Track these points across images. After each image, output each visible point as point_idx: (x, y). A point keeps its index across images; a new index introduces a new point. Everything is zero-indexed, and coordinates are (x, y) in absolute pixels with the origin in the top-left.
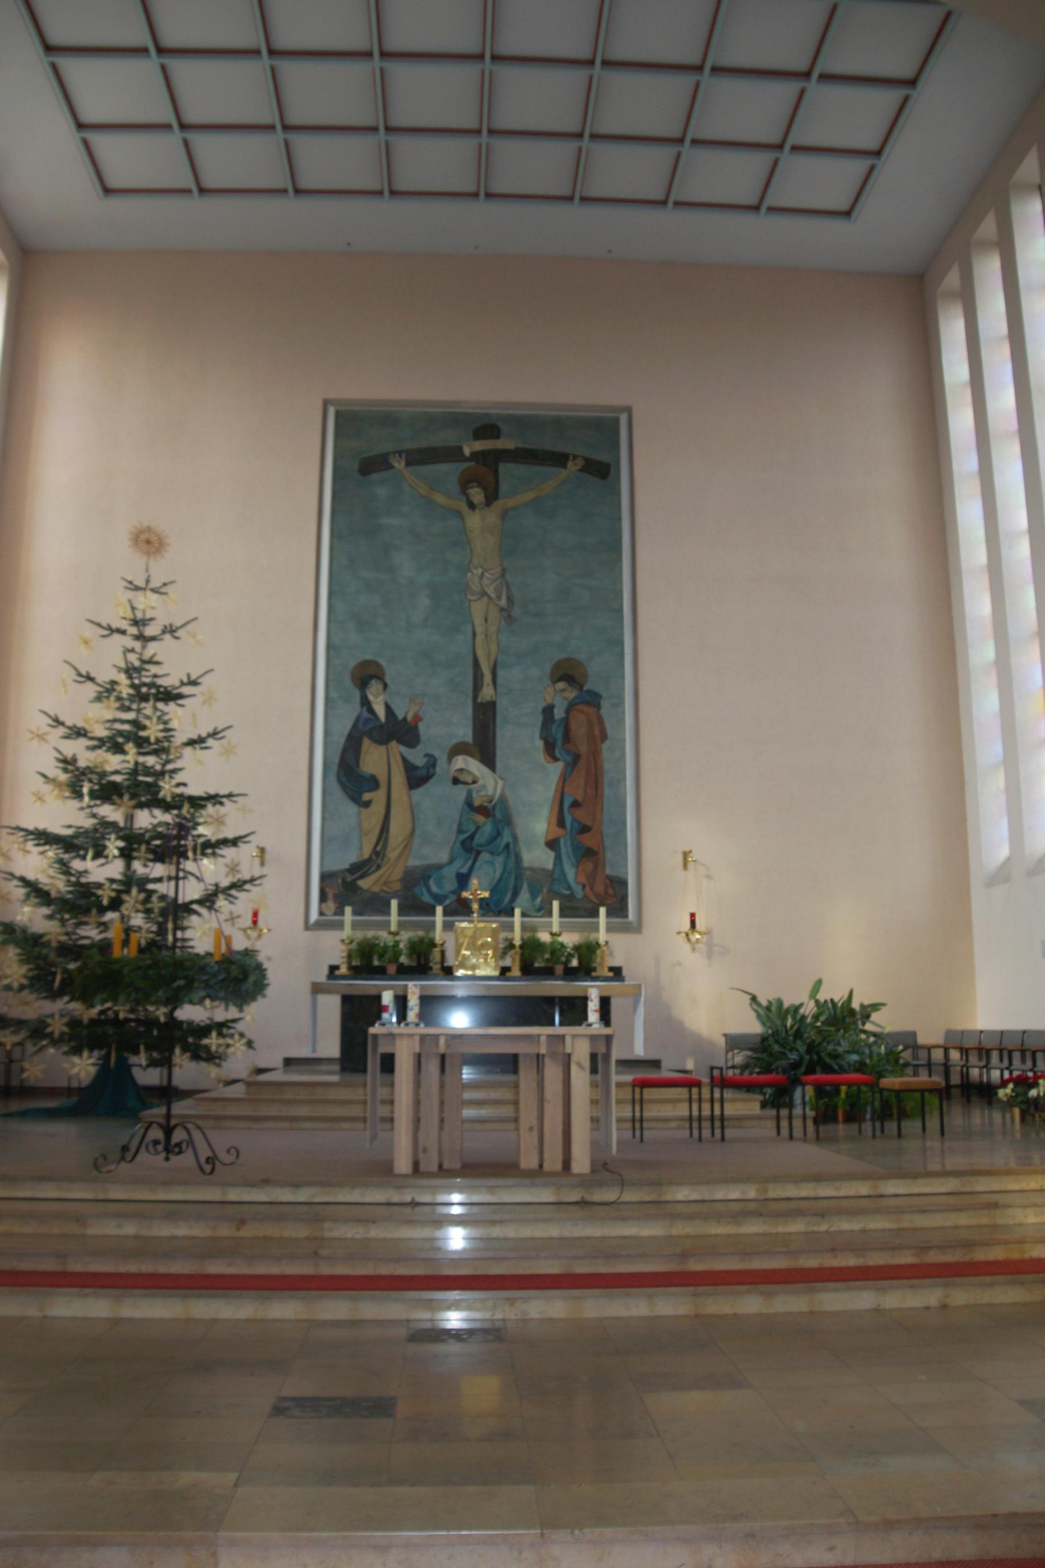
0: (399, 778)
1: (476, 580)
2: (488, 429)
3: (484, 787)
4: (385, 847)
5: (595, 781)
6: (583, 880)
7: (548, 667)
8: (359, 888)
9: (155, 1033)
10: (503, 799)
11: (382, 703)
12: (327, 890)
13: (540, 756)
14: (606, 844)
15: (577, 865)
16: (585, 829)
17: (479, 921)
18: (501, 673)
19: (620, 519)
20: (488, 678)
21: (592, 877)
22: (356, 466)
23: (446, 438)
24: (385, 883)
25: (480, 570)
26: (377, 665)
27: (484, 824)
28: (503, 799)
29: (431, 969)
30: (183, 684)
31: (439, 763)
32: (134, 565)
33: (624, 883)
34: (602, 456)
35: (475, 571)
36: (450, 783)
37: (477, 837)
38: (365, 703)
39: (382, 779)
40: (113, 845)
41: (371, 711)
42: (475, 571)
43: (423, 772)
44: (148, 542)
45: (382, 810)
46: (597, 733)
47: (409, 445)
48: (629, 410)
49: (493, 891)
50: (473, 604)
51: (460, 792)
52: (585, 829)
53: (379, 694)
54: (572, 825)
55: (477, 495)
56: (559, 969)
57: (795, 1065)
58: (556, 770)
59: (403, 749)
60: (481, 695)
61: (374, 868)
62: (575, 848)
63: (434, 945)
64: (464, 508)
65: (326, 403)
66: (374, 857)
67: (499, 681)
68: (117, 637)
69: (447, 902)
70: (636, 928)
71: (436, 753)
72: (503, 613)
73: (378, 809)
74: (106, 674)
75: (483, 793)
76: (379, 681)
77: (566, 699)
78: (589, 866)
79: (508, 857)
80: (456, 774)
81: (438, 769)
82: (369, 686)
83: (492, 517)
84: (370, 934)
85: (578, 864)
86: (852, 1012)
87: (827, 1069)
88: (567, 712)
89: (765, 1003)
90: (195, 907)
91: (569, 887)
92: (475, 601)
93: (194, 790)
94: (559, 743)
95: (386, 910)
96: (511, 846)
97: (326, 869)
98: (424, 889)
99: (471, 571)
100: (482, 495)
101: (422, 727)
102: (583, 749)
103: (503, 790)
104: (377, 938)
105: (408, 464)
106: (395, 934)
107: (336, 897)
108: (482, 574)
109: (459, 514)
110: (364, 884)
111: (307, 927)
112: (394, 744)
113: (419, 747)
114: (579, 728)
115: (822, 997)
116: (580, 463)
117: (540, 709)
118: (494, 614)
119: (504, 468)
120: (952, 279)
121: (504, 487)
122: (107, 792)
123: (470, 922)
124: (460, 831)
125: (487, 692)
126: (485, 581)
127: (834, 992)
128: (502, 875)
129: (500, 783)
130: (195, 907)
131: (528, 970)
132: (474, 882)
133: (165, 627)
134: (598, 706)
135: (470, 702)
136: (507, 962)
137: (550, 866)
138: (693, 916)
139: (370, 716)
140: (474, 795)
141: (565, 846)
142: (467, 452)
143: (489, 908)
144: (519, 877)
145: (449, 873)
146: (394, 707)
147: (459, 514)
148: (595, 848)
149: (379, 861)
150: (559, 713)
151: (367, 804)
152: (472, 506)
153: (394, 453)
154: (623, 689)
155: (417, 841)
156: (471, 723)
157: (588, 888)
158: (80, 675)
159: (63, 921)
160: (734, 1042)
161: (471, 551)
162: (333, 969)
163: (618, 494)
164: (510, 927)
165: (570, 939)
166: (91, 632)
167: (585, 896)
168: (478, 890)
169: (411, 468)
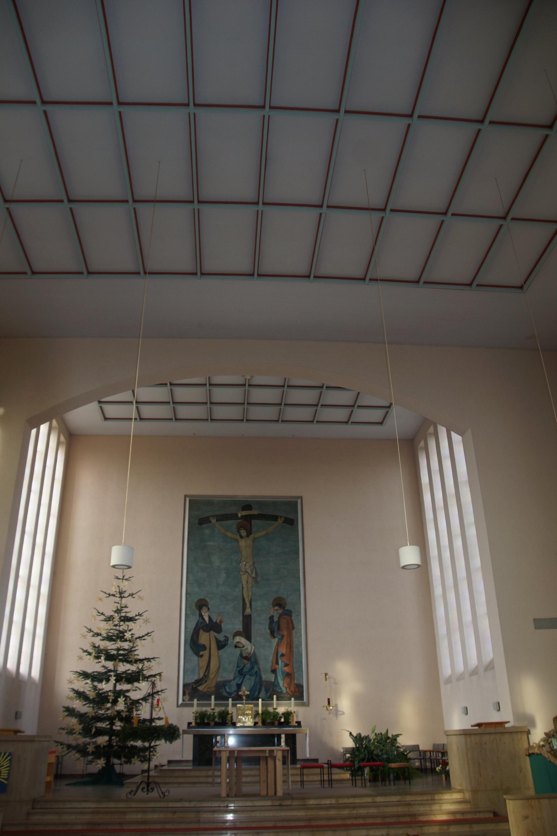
1: (243, 567)
2: (247, 506)
3: (247, 649)
4: (208, 673)
6: (286, 685)
7: (271, 601)
8: (198, 690)
9: (127, 751)
10: (254, 654)
11: (208, 615)
12: (186, 691)
13: (269, 636)
14: (295, 671)
17: (246, 704)
18: (253, 603)
19: (298, 541)
20: (248, 606)
22: (197, 522)
23: (231, 510)
24: (209, 688)
25: (245, 563)
27: (247, 663)
28: (254, 654)
29: (227, 723)
30: (136, 616)
31: (229, 639)
33: (302, 687)
34: (290, 517)
35: (243, 563)
36: (234, 648)
37: (244, 669)
38: (201, 616)
40: (113, 679)
41: (203, 619)
42: (243, 563)
47: (217, 513)
48: (301, 498)
49: (250, 691)
50: (242, 576)
51: (238, 651)
53: (206, 612)
54: (281, 663)
55: (244, 533)
56: (276, 723)
59: (215, 634)
60: (245, 612)
61: (204, 682)
63: (229, 714)
64: (238, 537)
65: (186, 496)
66: (204, 677)
67: (253, 607)
68: (111, 597)
69: (233, 695)
70: (307, 705)
71: (228, 636)
72: (254, 579)
73: (206, 658)
74: (109, 613)
75: (246, 651)
76: (206, 607)
77: (278, 613)
80: (236, 644)
81: (229, 642)
82: (203, 609)
83: (249, 541)
84: (204, 709)
85: (284, 679)
87: (374, 760)
88: (279, 618)
90: (141, 701)
91: (281, 689)
92: (244, 574)
93: (141, 657)
94: (276, 631)
95: (210, 699)
96: (258, 672)
97: (185, 682)
98: (224, 690)
99: (242, 563)
100: (246, 533)
101: (223, 625)
102: (285, 633)
103: (254, 650)
104: (206, 711)
105: (217, 521)
106: (213, 709)
108: (246, 564)
109: (237, 540)
110: (200, 688)
111: (178, 706)
112: (212, 632)
113: (222, 633)
115: (377, 731)
116: (283, 519)
117: (268, 617)
118: (250, 580)
119: (253, 522)
120: (422, 444)
121: (254, 529)
122: (110, 657)
123: (242, 704)
124: (238, 667)
125: (248, 611)
126: (247, 567)
128: (254, 684)
129: (253, 647)
130: (141, 701)
132: (244, 688)
133: (130, 594)
134: (291, 616)
135: (241, 615)
136: (257, 720)
137: (273, 680)
138: (329, 699)
139: (203, 621)
140: (243, 652)
142: (239, 515)
143: (249, 698)
144: (261, 685)
145: (234, 683)
146: (212, 617)
147: (237, 540)
149: (206, 679)
150: (276, 619)
151: (202, 656)
152: (242, 537)
153: (212, 516)
154: (300, 609)
155: (221, 671)
156: (241, 623)
157: (288, 689)
158: (99, 612)
159: (93, 707)
161: (241, 555)
162: (189, 724)
163: (297, 531)
164: (257, 705)
166: (103, 595)
167: (287, 692)
168: (245, 691)
169: (218, 522)
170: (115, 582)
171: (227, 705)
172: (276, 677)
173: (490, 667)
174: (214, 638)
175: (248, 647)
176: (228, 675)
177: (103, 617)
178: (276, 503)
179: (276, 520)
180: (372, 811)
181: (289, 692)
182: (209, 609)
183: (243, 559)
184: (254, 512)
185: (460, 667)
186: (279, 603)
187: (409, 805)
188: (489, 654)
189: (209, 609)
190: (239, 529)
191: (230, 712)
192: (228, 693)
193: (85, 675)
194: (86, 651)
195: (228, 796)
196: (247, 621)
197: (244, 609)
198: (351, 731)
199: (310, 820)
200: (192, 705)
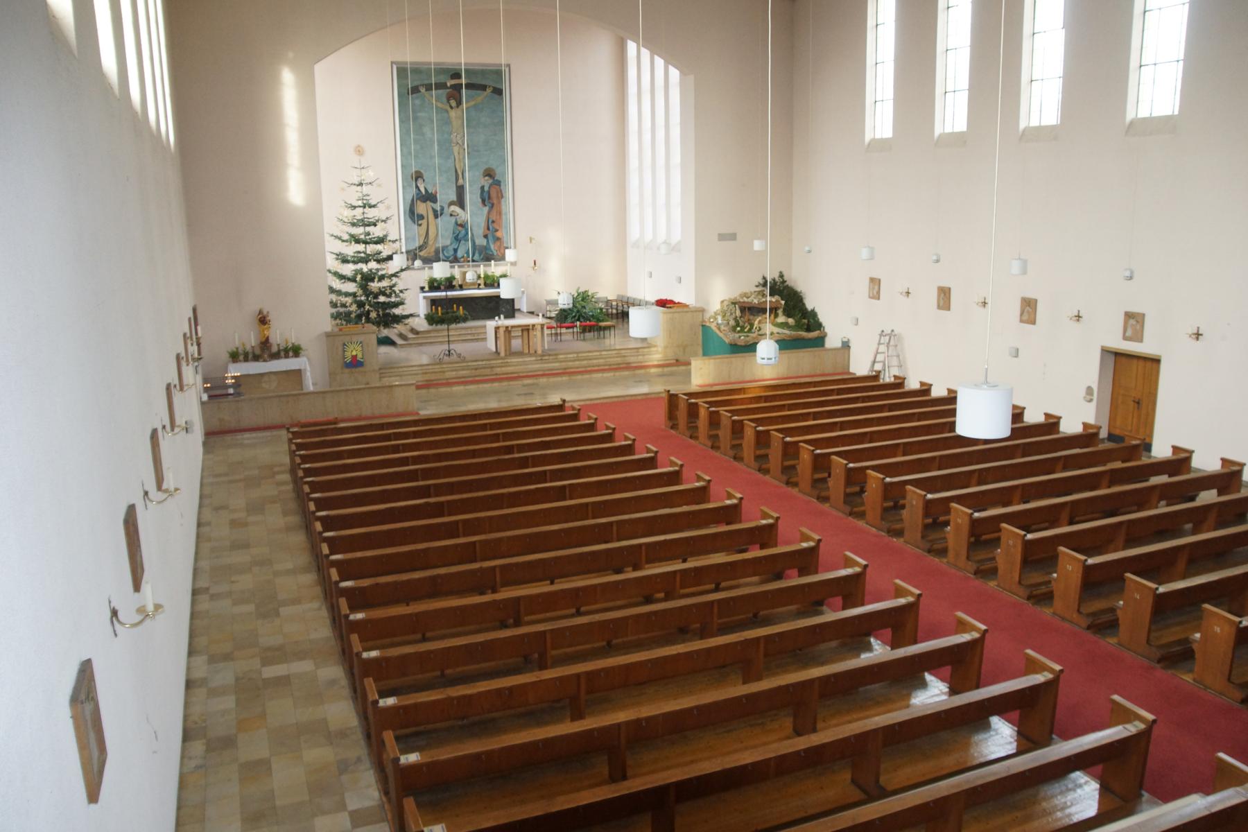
3: (461, 217)
4: (427, 240)
5: (500, 213)
6: (496, 248)
7: (482, 171)
15: (494, 243)
16: (497, 231)
34: (498, 86)
38: (417, 187)
39: (425, 215)
41: (419, 190)
44: (359, 151)
45: (426, 227)
46: (500, 195)
51: (453, 219)
55: (453, 103)
57: (575, 316)
58: (486, 209)
59: (432, 204)
62: (494, 236)
64: (449, 109)
65: (392, 63)
69: (450, 259)
71: (444, 205)
73: (425, 226)
88: (489, 188)
91: (492, 251)
102: (495, 201)
105: (426, 90)
109: (447, 111)
110: (422, 254)
112: (428, 202)
114: (493, 194)
115: (579, 291)
116: (491, 89)
124: (454, 233)
125: (461, 182)
134: (500, 186)
137: (485, 244)
142: (449, 85)
145: (451, 248)
147: (447, 111)
148: (500, 237)
150: (486, 189)
151: (420, 225)
152: (452, 108)
172: (488, 241)
173: (675, 249)
174: (431, 209)
178: (484, 72)
179: (485, 90)
180: (601, 361)
181: (499, 254)
182: (424, 181)
183: (454, 130)
186: (489, 173)
187: (625, 356)
188: (677, 236)
189: (424, 181)
190: (448, 100)
192: (446, 257)
194: (332, 235)
195: (506, 355)
196: (460, 191)
197: (457, 179)
199: (565, 369)
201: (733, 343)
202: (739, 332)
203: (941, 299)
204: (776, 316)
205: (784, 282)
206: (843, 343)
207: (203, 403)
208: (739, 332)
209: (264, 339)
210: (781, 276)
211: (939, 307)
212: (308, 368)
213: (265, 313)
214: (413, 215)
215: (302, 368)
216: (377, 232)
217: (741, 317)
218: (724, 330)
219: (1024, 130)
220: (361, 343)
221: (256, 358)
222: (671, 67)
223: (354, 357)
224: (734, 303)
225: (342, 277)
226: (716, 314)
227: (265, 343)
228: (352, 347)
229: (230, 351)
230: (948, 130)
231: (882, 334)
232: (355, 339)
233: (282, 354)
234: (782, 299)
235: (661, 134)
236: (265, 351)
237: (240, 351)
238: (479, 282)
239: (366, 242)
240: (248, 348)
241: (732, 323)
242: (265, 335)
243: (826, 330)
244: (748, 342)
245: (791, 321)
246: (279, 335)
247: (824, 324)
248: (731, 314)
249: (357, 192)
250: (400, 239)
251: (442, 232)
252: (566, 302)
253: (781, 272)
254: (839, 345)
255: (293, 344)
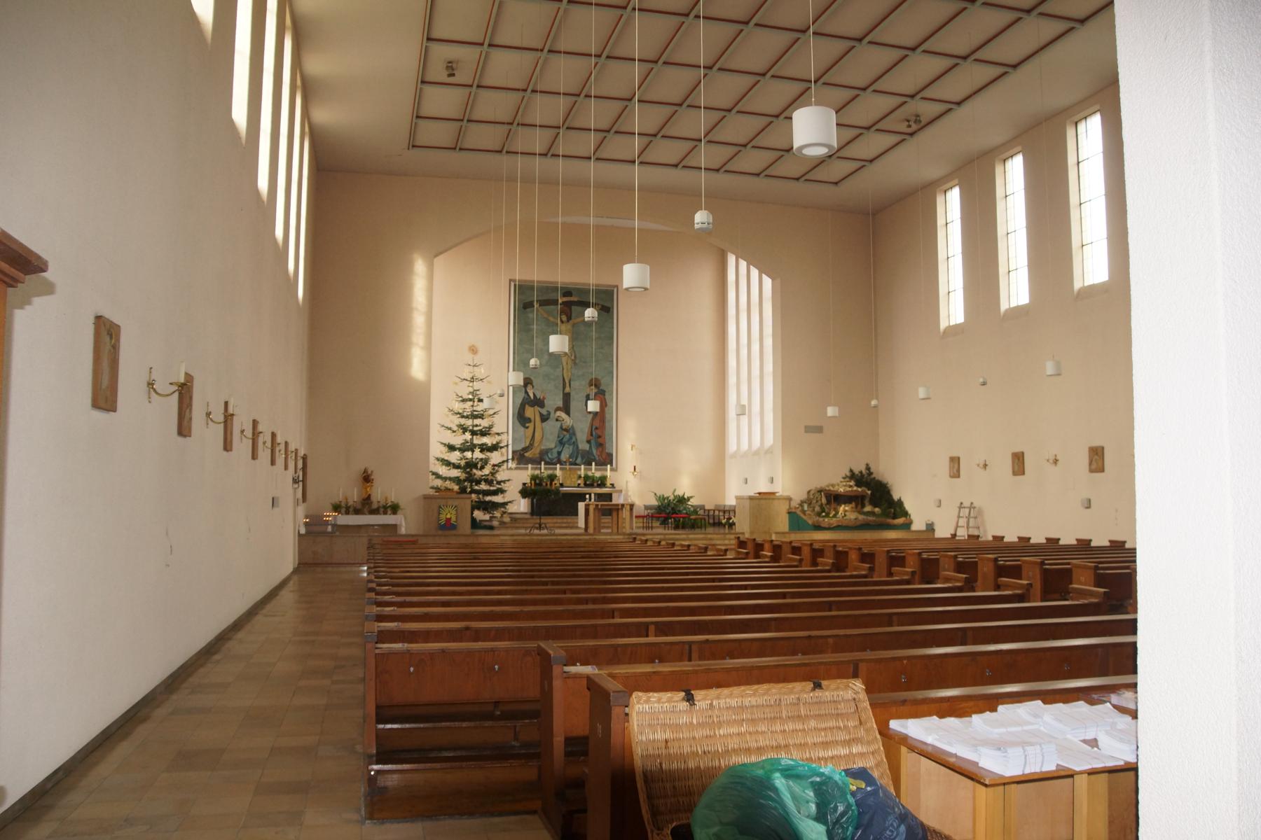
0: (538, 419)
2: (567, 293)
4: (533, 443)
6: (599, 453)
7: (588, 382)
10: (572, 426)
15: (597, 448)
16: (600, 437)
18: (572, 383)
20: (568, 385)
21: (601, 452)
26: (530, 379)
28: (572, 426)
32: (469, 357)
33: (612, 455)
38: (526, 392)
39: (533, 419)
41: (528, 395)
43: (546, 417)
44: (473, 350)
45: (533, 429)
51: (558, 424)
52: (600, 437)
55: (564, 318)
59: (539, 409)
62: (596, 443)
71: (550, 410)
78: (601, 449)
79: (574, 447)
83: (569, 326)
84: (537, 472)
86: (685, 499)
89: (658, 495)
97: (514, 449)
101: (545, 401)
107: (517, 459)
110: (526, 454)
112: (536, 407)
115: (675, 494)
116: (600, 306)
118: (570, 362)
119: (574, 308)
121: (573, 315)
124: (558, 437)
125: (567, 390)
127: (679, 493)
131: (586, 485)
134: (604, 395)
137: (588, 449)
138: (635, 467)
141: (593, 442)
144: (578, 453)
145: (555, 451)
151: (527, 428)
152: (562, 322)
160: (647, 508)
165: (598, 474)
170: (468, 369)
171: (556, 469)
173: (769, 451)
175: (568, 421)
176: (550, 443)
177: (461, 399)
184: (574, 299)
185: (745, 446)
188: (770, 440)
191: (558, 475)
192: (550, 459)
193: (452, 448)
194: (443, 426)
196: (567, 398)
197: (564, 387)
198: (655, 492)
200: (527, 469)
201: (817, 525)
202: (823, 517)
203: (1015, 464)
204: (863, 506)
205: (871, 474)
206: (927, 525)
207: (300, 535)
208: (823, 517)
209: (365, 496)
210: (868, 468)
211: (1015, 473)
212: (404, 524)
213: (369, 472)
214: (521, 418)
215: (398, 523)
216: (484, 423)
217: (827, 504)
218: (810, 515)
219: (1080, 290)
220: (455, 507)
221: (357, 512)
222: (764, 276)
223: (448, 520)
224: (820, 491)
225: (447, 463)
226: (802, 502)
227: (367, 500)
228: (447, 510)
229: (333, 502)
230: (1013, 305)
231: (961, 506)
232: (450, 502)
233: (382, 510)
234: (869, 490)
235: (756, 347)
236: (366, 505)
237: (343, 504)
238: (579, 482)
239: (473, 433)
240: (351, 503)
241: (817, 509)
242: (367, 492)
243: (912, 517)
244: (833, 524)
245: (877, 510)
246: (379, 493)
247: (910, 512)
248: (817, 501)
249: (469, 386)
250: (508, 432)
251: (547, 436)
252: (590, 316)
253: (867, 465)
254: (924, 528)
255: (392, 502)
